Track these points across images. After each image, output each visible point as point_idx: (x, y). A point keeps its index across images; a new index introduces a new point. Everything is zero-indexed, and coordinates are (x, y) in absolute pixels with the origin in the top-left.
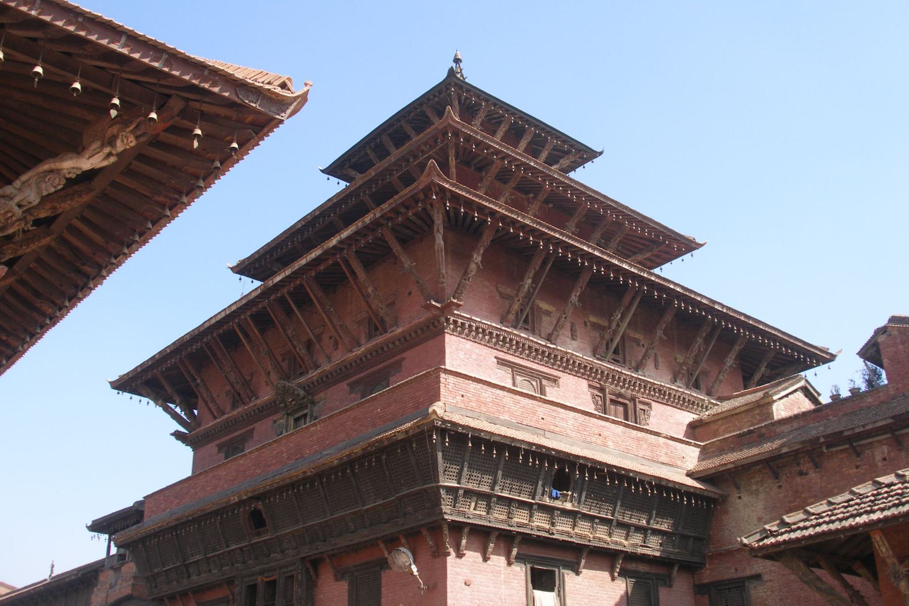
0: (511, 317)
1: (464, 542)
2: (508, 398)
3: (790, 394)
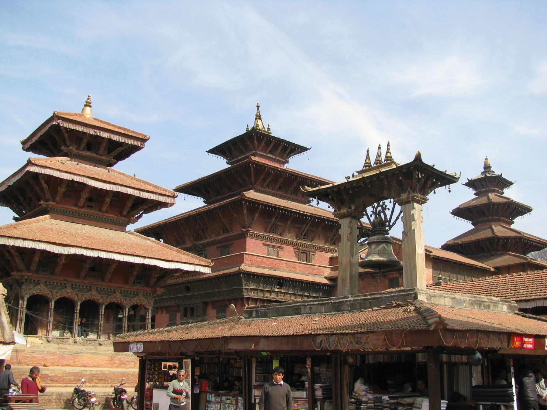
0: (268, 230)
1: (250, 302)
2: (265, 260)
3: (363, 251)
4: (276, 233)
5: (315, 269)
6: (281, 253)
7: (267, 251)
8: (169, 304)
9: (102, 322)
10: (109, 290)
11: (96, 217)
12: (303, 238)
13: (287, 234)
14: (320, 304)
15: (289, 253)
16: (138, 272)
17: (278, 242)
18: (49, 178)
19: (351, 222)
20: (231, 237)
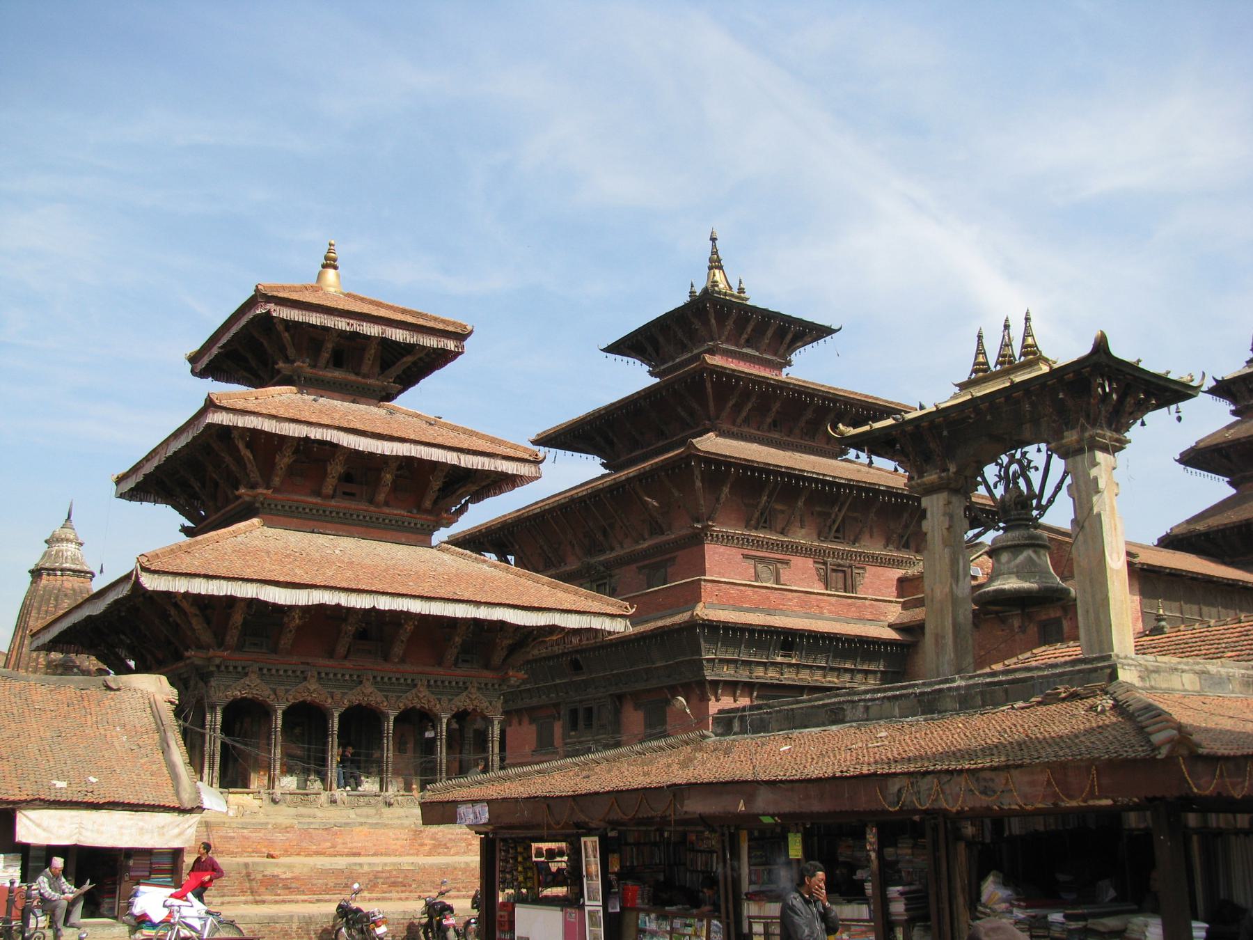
1: (720, 691)
2: (749, 591)
4: (771, 528)
5: (865, 607)
6: (785, 574)
8: (534, 702)
9: (391, 755)
10: (402, 681)
11: (364, 517)
12: (835, 538)
13: (798, 530)
14: (889, 698)
15: (803, 574)
16: (464, 637)
17: (777, 550)
18: (255, 435)
19: (949, 503)
20: (669, 544)
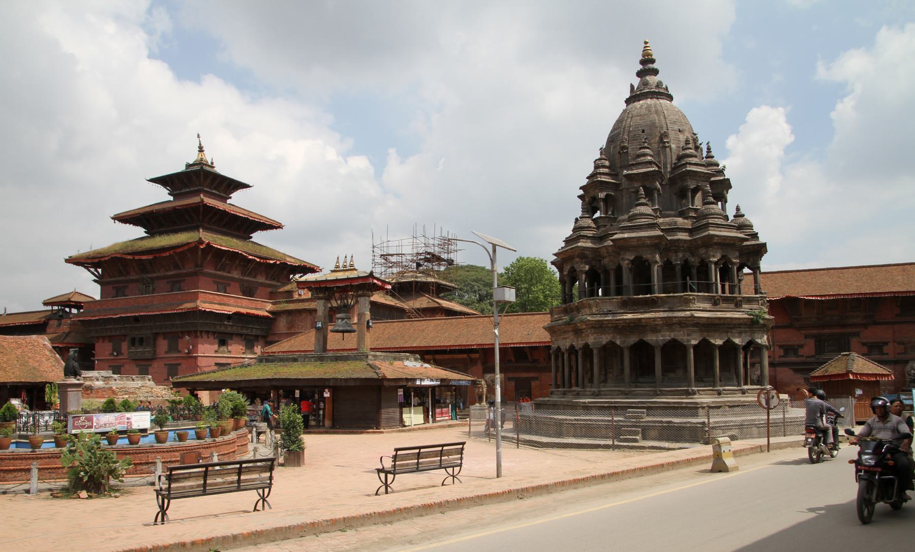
2: (217, 297)
6: (228, 289)
7: (216, 287)
8: (114, 333)
19: (325, 303)
